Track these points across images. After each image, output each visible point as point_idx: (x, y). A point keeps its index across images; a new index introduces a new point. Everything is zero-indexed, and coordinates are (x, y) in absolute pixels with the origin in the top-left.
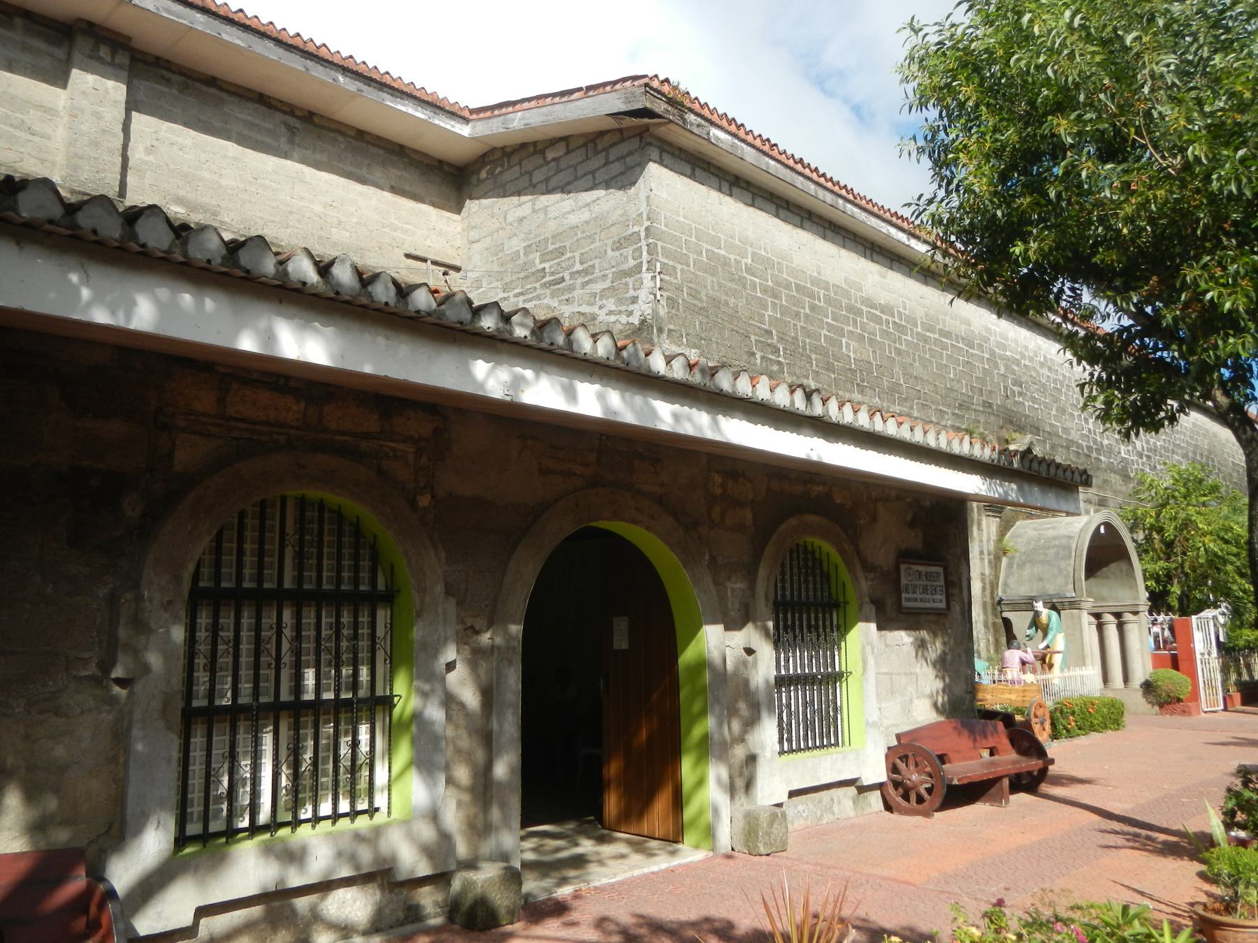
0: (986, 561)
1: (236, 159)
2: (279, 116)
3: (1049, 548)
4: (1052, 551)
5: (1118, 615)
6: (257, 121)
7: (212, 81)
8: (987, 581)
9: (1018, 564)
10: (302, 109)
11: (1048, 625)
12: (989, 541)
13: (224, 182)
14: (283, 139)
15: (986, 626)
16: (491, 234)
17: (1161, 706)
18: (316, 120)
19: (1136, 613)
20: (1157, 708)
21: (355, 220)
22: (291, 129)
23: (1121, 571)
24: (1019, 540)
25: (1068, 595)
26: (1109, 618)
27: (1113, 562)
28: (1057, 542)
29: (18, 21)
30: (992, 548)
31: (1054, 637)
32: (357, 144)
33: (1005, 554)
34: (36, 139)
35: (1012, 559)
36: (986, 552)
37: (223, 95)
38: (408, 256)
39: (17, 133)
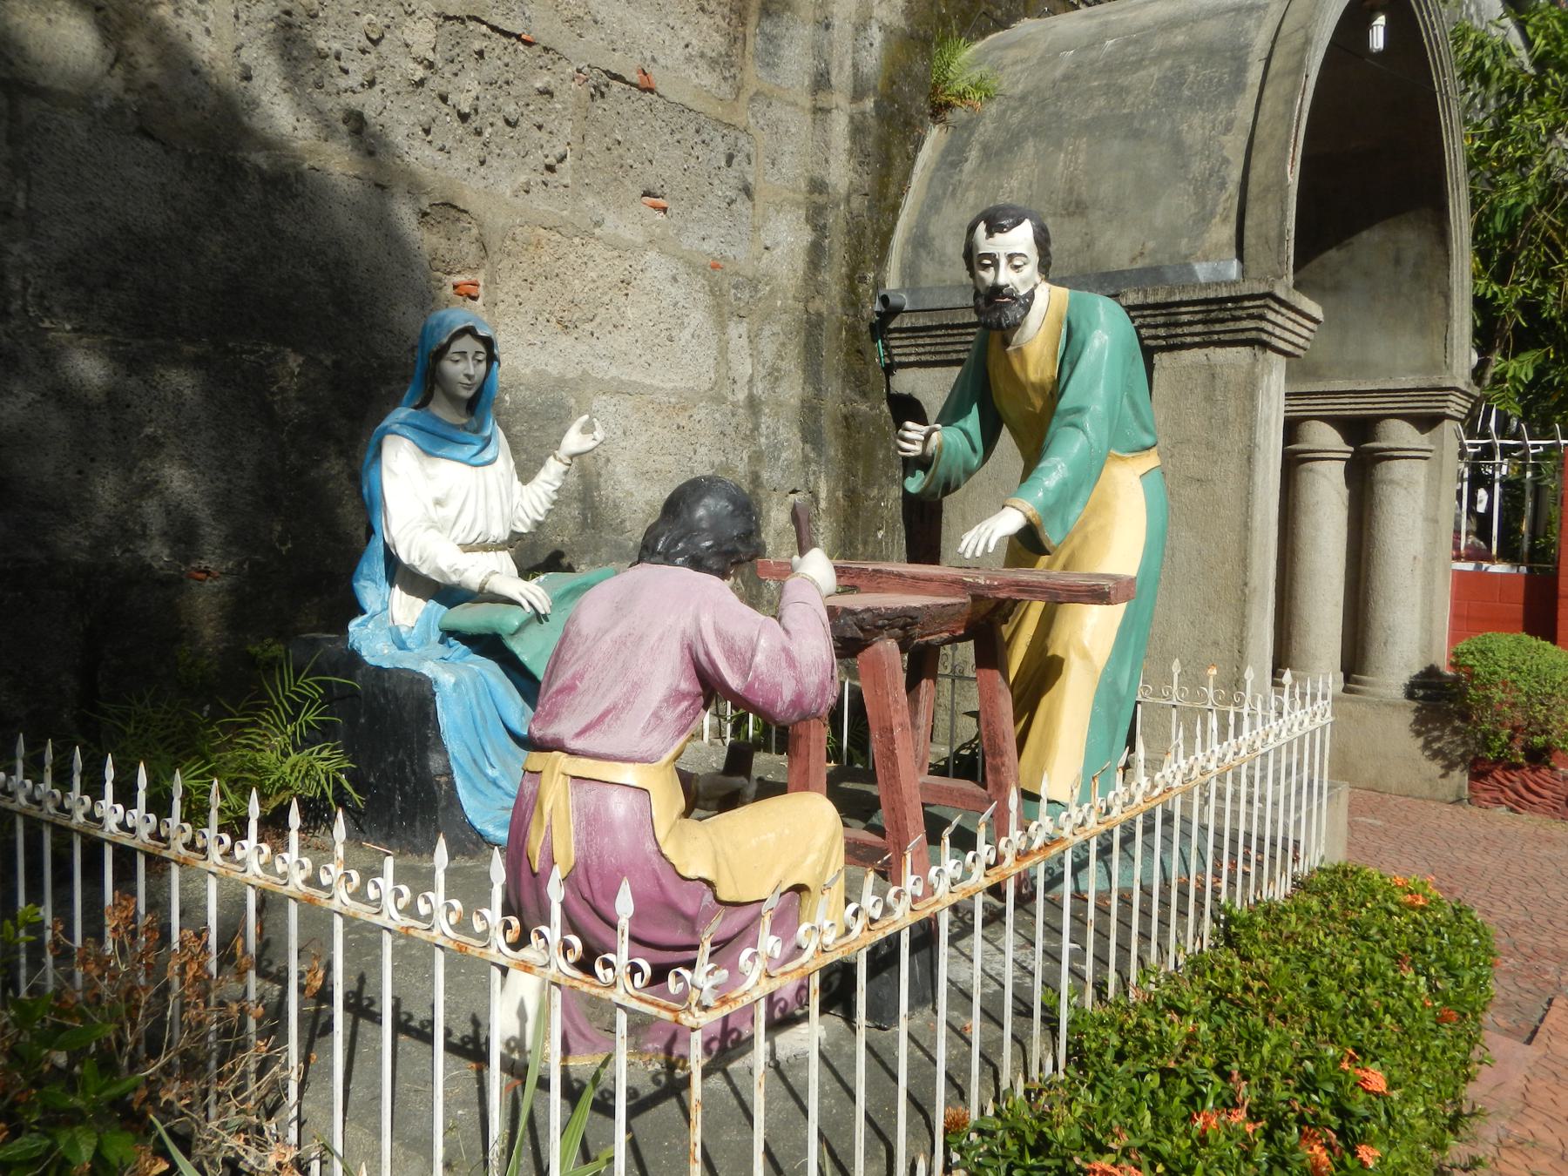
0: (840, 125)
3: (1138, 64)
4: (1155, 72)
5: (1358, 430)
8: (836, 220)
9: (986, 148)
11: (1055, 391)
12: (861, 27)
15: (811, 435)
17: (1479, 773)
19: (1427, 422)
20: (1460, 777)
23: (1398, 261)
24: (1011, 54)
25: (1202, 271)
26: (1325, 437)
27: (1368, 223)
28: (1180, 38)
30: (872, 60)
31: (1088, 475)
33: (939, 110)
35: (969, 126)
36: (841, 78)
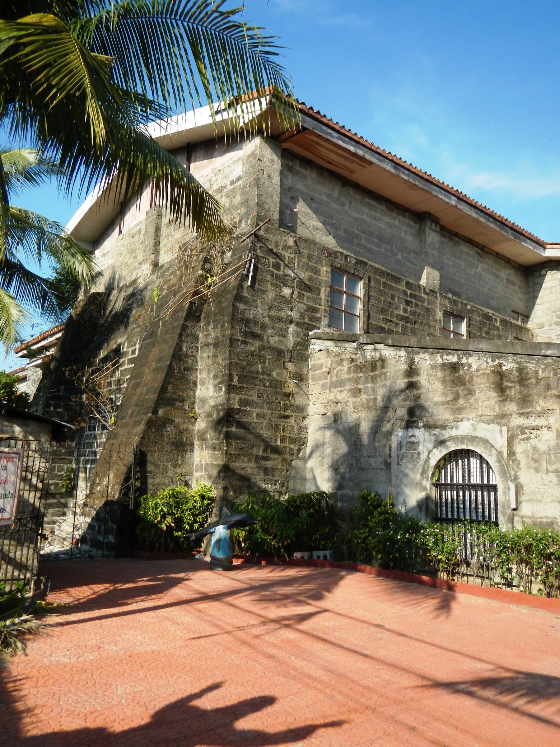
1: (464, 270)
2: (475, 249)
6: (469, 252)
7: (456, 235)
10: (481, 245)
13: (463, 281)
14: (476, 259)
16: (551, 302)
18: (485, 249)
21: (497, 296)
22: (478, 254)
29: (407, 214)
32: (497, 259)
34: (413, 266)
37: (460, 241)
38: (513, 311)
39: (409, 264)
